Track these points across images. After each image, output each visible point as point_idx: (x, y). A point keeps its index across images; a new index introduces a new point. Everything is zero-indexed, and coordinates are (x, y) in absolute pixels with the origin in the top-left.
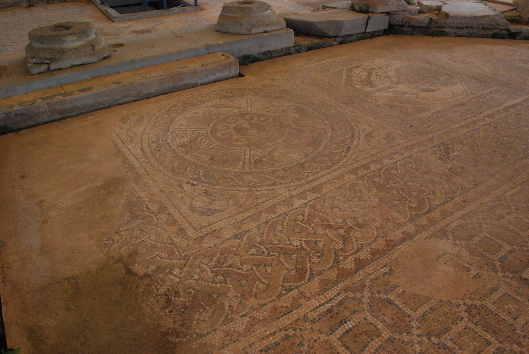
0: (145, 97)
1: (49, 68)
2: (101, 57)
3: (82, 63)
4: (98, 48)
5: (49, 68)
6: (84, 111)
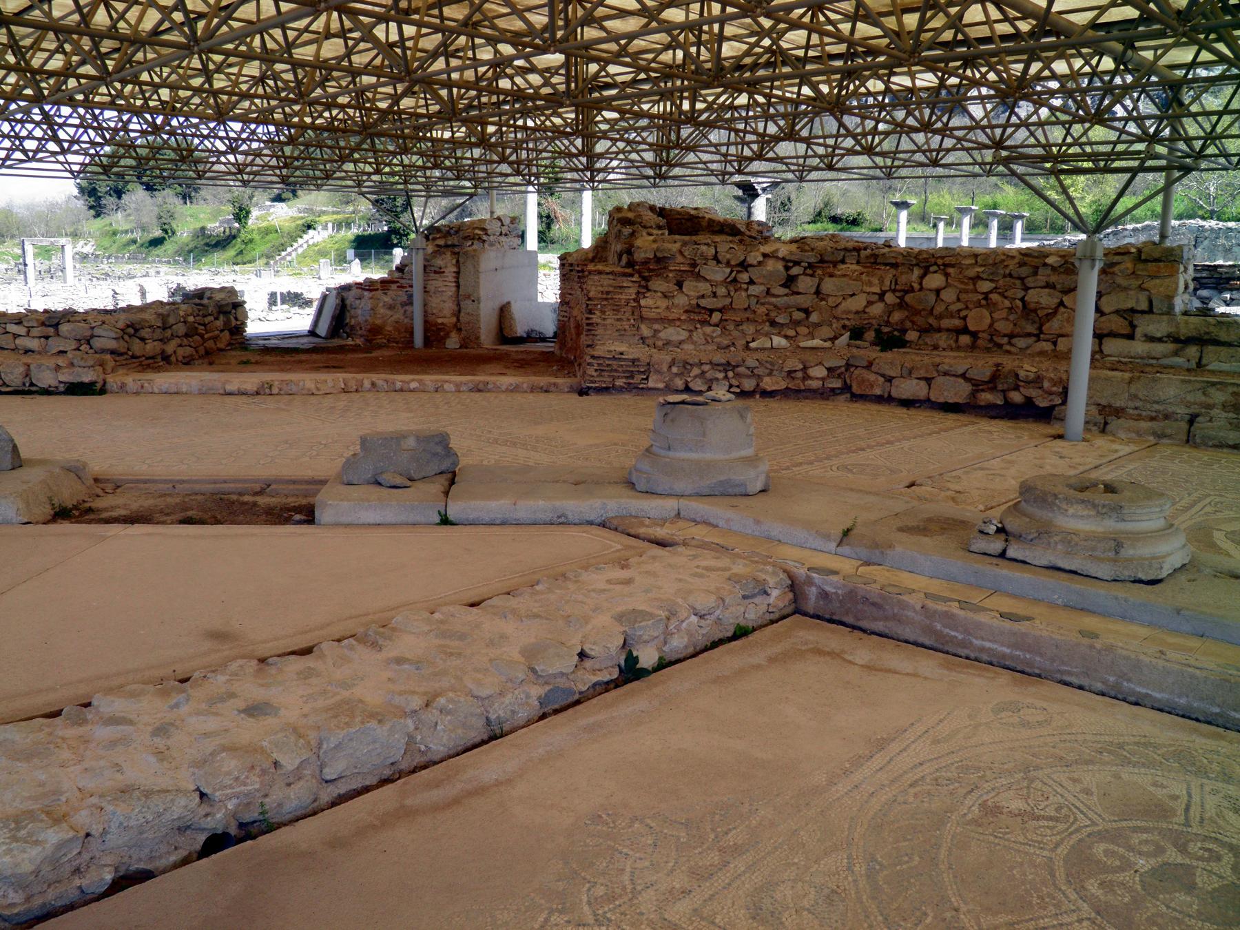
0: (1133, 699)
1: (1004, 551)
2: (1126, 574)
3: (1073, 568)
4: (1128, 552)
5: (1004, 551)
6: (985, 657)
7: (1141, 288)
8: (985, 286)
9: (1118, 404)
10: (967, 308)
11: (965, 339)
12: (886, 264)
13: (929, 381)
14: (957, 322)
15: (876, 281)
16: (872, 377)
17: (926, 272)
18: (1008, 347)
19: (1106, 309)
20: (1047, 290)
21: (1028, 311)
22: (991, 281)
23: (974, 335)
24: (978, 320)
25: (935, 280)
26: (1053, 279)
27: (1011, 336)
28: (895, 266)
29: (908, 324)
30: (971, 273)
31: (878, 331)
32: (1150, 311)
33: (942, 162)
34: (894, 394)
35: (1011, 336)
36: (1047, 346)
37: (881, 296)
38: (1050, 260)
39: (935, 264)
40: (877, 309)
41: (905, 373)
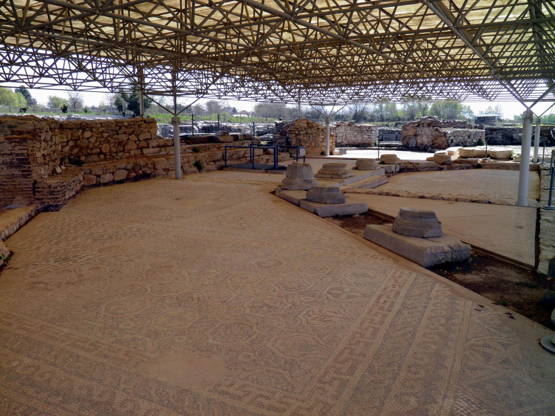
7: (149, 131)
8: (106, 135)
9: (167, 167)
10: (101, 144)
11: (102, 156)
12: (67, 129)
13: (113, 173)
14: (98, 150)
15: (65, 137)
16: (93, 177)
17: (84, 130)
18: (116, 157)
19: (141, 139)
20: (124, 135)
21: (120, 143)
22: (107, 133)
23: (105, 154)
24: (105, 148)
25: (88, 134)
26: (126, 130)
27: (117, 153)
28: (71, 129)
29: (81, 154)
30: (101, 130)
31: (69, 159)
32: (151, 139)
33: (11, 79)
34: (102, 181)
35: (117, 153)
36: (128, 154)
37: (68, 142)
38: (125, 124)
39: (88, 127)
40: (67, 149)
41: (105, 172)
